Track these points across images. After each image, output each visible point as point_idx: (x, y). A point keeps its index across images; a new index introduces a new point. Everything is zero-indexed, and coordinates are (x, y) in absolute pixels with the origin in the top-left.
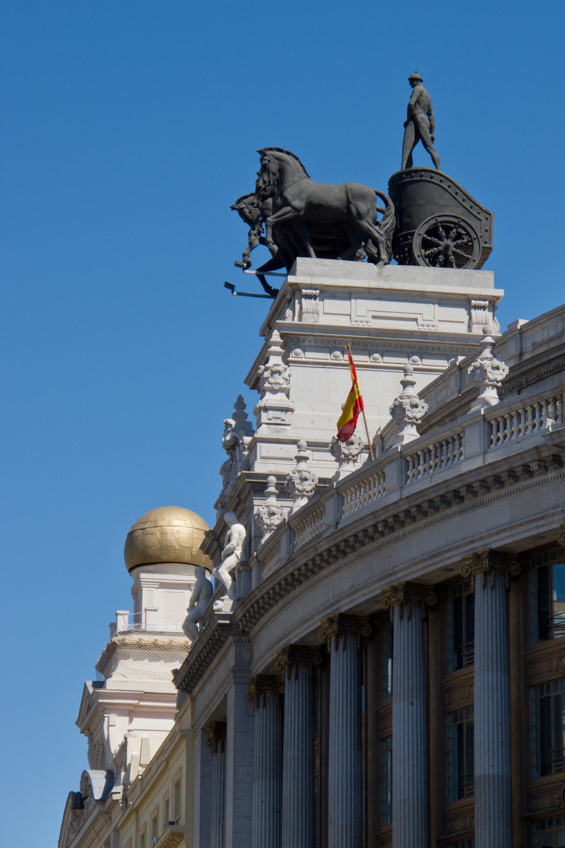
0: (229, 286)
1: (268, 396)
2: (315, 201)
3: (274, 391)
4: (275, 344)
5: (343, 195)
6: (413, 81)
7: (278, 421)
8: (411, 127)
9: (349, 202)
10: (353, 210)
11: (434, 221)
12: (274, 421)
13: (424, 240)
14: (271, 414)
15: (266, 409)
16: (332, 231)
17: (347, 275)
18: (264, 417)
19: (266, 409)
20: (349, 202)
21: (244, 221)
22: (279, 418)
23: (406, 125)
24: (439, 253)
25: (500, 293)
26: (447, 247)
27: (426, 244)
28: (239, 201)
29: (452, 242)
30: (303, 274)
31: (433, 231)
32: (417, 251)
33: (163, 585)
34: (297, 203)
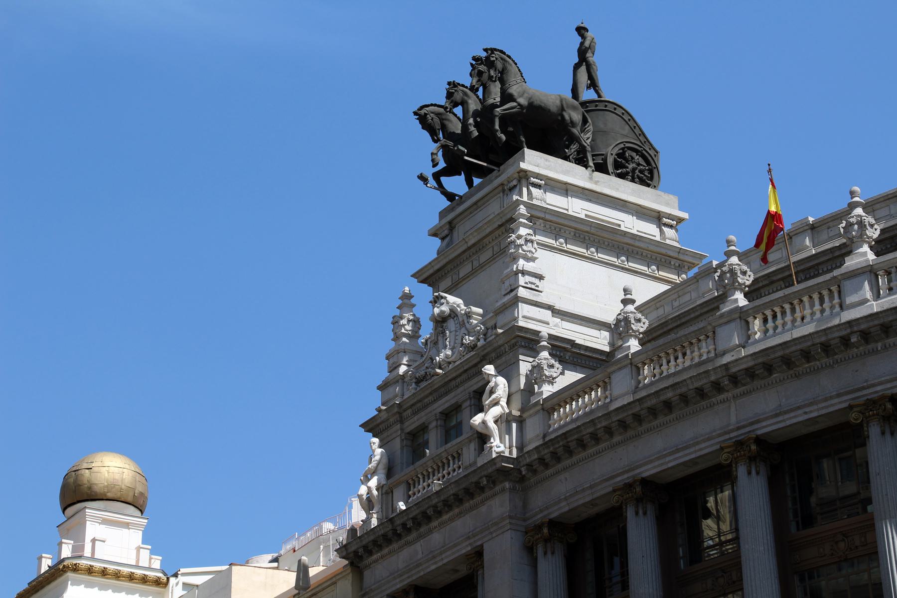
0: (422, 178)
1: (521, 262)
2: (537, 103)
3: (528, 259)
4: (523, 216)
5: (558, 102)
7: (533, 287)
9: (562, 109)
10: (567, 117)
11: (622, 146)
12: (529, 286)
13: (615, 160)
14: (528, 278)
15: (524, 273)
16: (549, 131)
17: (566, 173)
18: (522, 280)
19: (524, 273)
20: (563, 109)
21: (423, 128)
22: (534, 284)
23: (576, 67)
24: (627, 173)
25: (685, 215)
26: (634, 170)
27: (617, 165)
28: (422, 108)
30: (530, 163)
31: (621, 155)
32: (610, 168)
33: (105, 522)
34: (523, 101)
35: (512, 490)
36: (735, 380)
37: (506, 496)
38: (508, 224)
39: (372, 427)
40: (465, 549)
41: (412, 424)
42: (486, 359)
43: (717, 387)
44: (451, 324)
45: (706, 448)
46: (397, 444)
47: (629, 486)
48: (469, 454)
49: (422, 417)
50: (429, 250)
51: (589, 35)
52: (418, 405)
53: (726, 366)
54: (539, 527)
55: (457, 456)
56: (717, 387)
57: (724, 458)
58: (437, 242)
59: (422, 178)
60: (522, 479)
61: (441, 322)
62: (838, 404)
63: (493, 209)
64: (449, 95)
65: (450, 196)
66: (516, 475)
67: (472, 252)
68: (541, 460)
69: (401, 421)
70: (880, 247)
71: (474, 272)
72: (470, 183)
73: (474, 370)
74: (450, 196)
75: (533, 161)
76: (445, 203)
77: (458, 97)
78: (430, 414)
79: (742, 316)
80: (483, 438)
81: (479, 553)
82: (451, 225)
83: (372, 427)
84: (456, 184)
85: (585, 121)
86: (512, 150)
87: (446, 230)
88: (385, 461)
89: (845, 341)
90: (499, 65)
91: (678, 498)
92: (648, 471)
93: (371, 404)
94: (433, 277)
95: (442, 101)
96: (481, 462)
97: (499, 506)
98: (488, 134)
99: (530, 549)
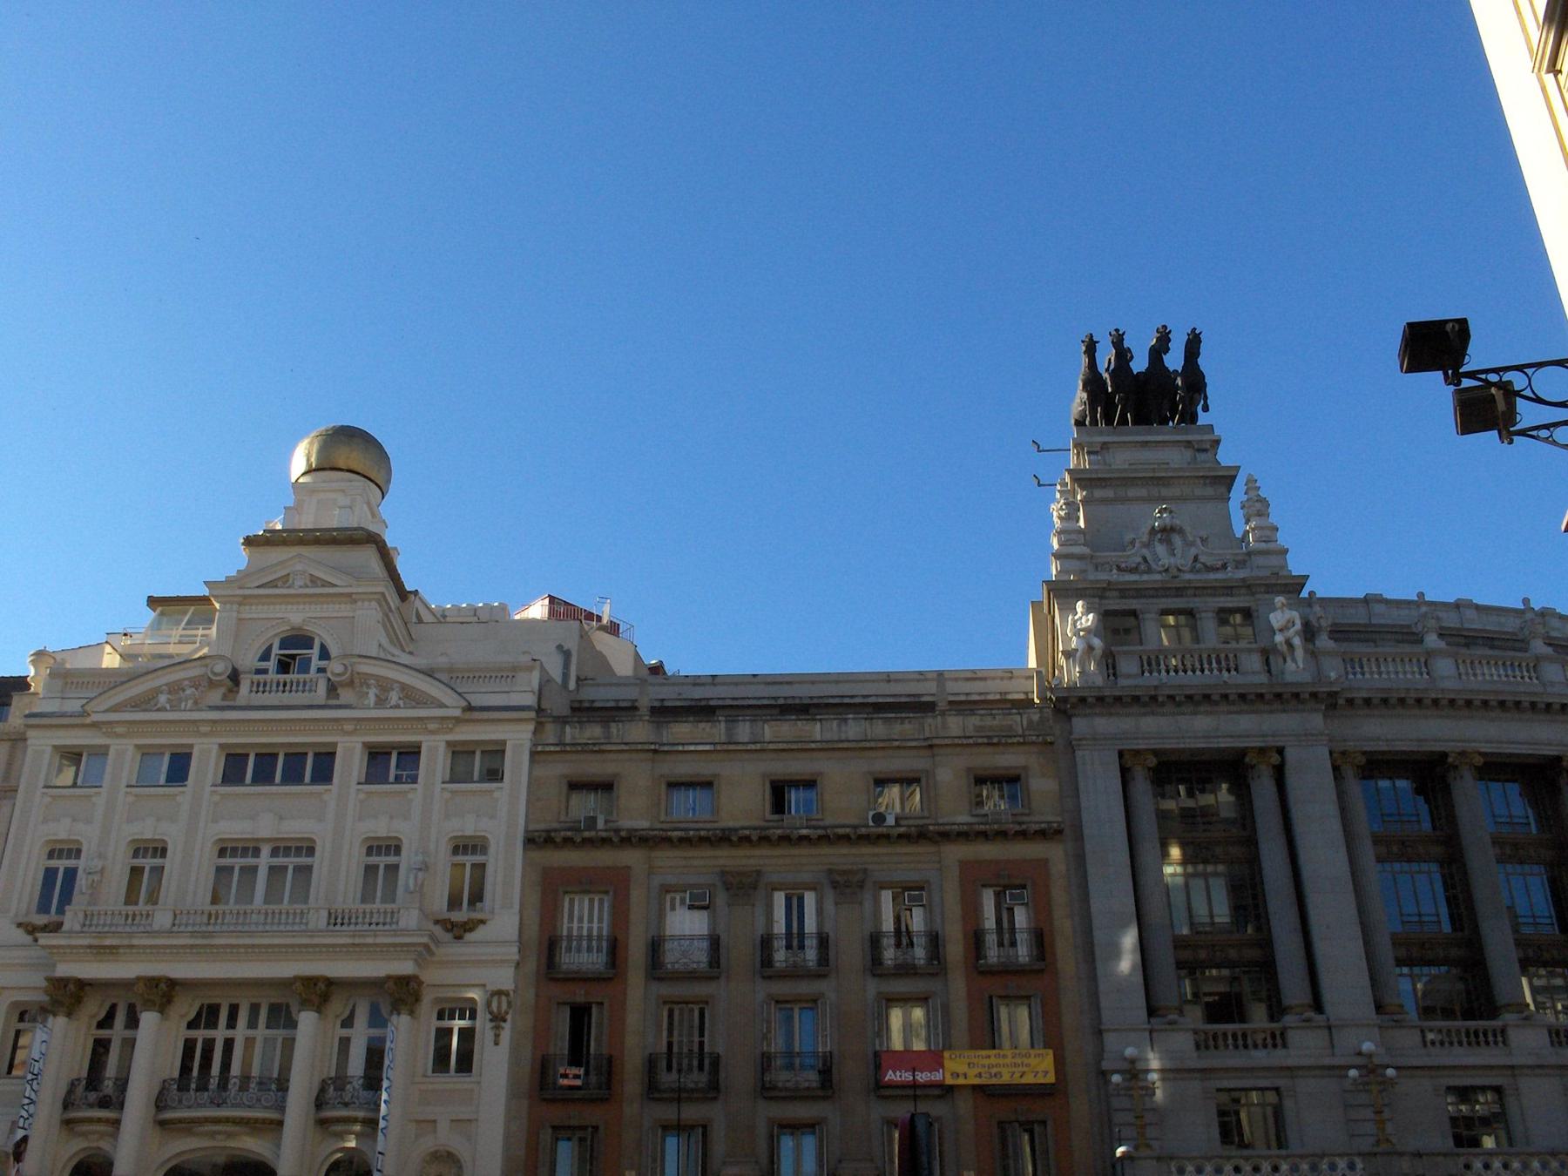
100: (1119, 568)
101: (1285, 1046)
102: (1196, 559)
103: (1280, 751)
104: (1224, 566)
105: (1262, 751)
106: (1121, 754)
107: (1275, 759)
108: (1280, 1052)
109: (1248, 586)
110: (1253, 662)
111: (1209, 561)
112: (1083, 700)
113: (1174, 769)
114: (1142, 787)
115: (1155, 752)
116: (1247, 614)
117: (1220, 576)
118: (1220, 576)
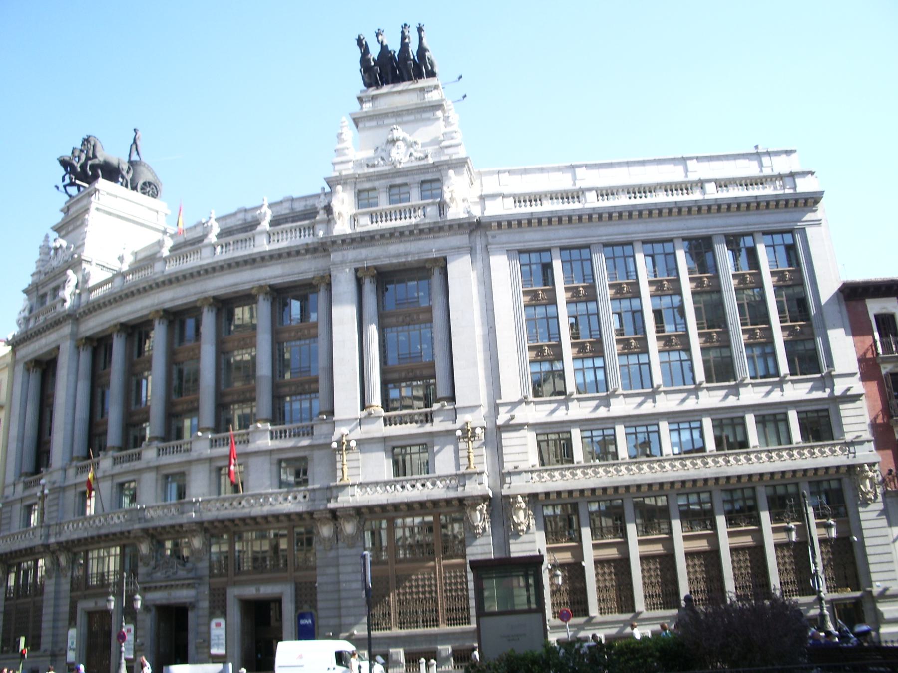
0: (57, 187)
6: (135, 130)
8: (134, 146)
16: (111, 172)
27: (142, 189)
29: (150, 189)
31: (144, 184)
35: (73, 323)
36: (157, 285)
37: (70, 326)
38: (86, 210)
39: (26, 291)
40: (54, 346)
41: (42, 292)
42: (69, 268)
43: (151, 287)
44: (60, 251)
45: (145, 312)
46: (35, 300)
47: (115, 325)
48: (59, 307)
49: (43, 289)
50: (59, 217)
51: (139, 133)
52: (44, 284)
53: (154, 280)
54: (82, 339)
55: (55, 307)
56: (151, 287)
57: (150, 317)
58: (62, 215)
59: (57, 187)
60: (77, 319)
61: (56, 249)
62: (193, 298)
63: (85, 202)
64: (73, 152)
65: (70, 196)
66: (74, 317)
67: (71, 222)
68: (84, 312)
69: (38, 290)
70: (219, 236)
71: (74, 230)
72: (79, 190)
73: (63, 272)
74: (70, 196)
75: (102, 184)
76: (68, 198)
77: (77, 153)
78: (48, 289)
79: (165, 260)
80: (64, 301)
81: (58, 348)
82: (68, 208)
83: (26, 291)
84: (73, 191)
85: (129, 168)
86: (95, 178)
87: (67, 210)
88: (29, 306)
89: (199, 273)
90: (93, 143)
91: (136, 331)
92: (123, 320)
93: (27, 281)
94: (58, 229)
95: (70, 154)
96: (62, 310)
97: (67, 329)
98: (86, 170)
99: (78, 348)
100: (368, 165)
101: (432, 421)
102: (411, 154)
103: (445, 259)
104: (426, 156)
105: (435, 260)
106: (357, 270)
107: (442, 264)
108: (429, 425)
109: (436, 166)
110: (432, 211)
111: (416, 154)
112: (334, 243)
113: (384, 277)
114: (369, 288)
115: (375, 267)
116: (438, 180)
117: (422, 162)
118: (422, 162)
